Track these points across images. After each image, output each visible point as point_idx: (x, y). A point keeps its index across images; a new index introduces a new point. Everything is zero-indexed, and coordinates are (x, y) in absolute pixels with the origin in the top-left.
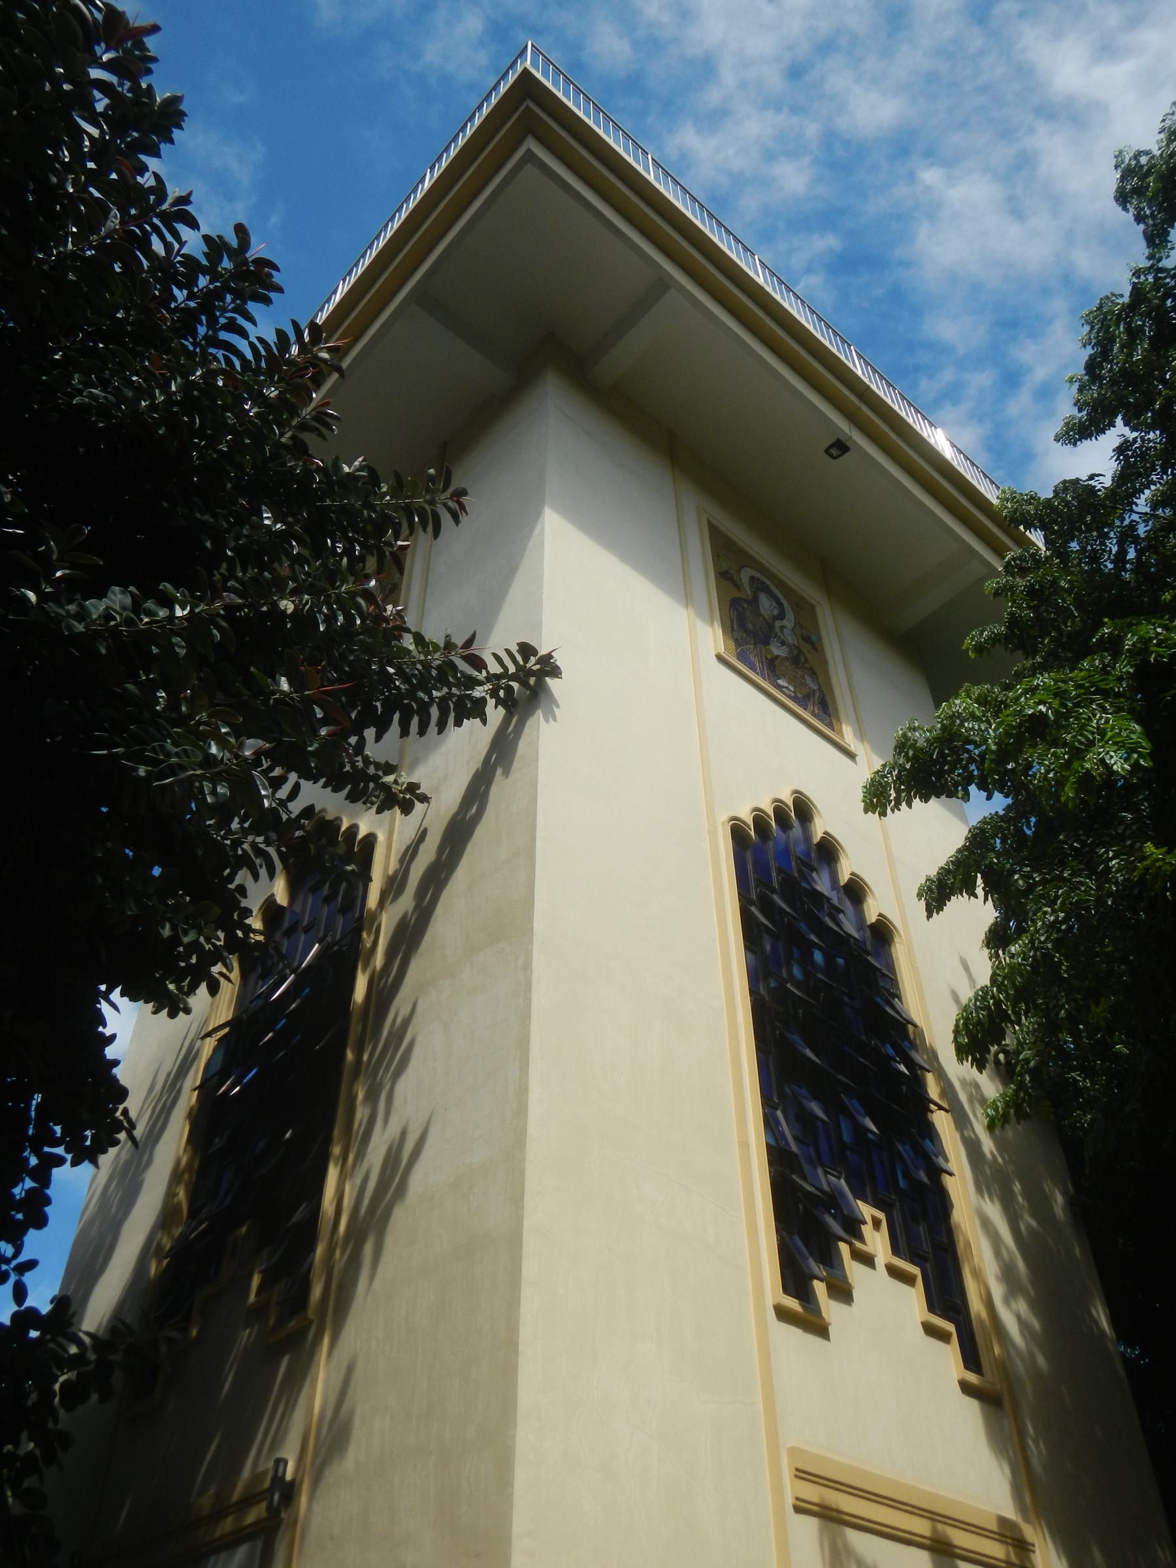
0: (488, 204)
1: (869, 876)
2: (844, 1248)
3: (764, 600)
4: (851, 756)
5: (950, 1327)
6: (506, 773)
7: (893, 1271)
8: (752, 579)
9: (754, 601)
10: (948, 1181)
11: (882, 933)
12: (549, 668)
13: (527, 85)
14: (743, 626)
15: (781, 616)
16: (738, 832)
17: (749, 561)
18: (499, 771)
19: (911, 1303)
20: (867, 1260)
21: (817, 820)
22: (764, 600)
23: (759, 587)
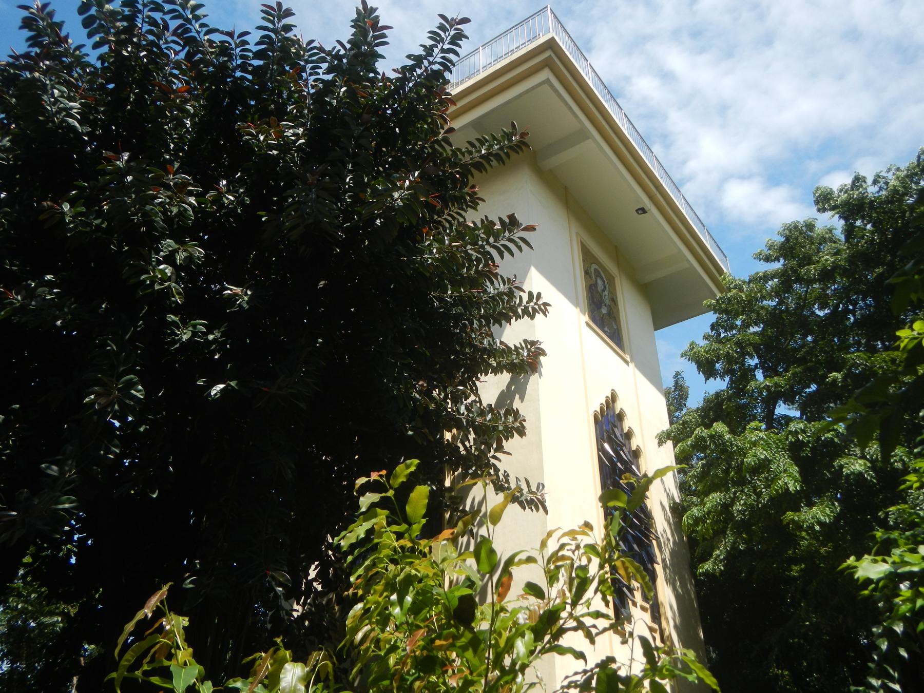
0: (521, 95)
1: (636, 431)
2: (630, 602)
3: (599, 282)
4: (627, 363)
5: (656, 627)
6: (522, 399)
7: (643, 608)
8: (595, 270)
9: (596, 285)
10: (655, 565)
11: (636, 454)
12: (541, 352)
13: (551, 44)
14: (593, 302)
15: (604, 290)
16: (596, 417)
17: (596, 261)
18: (517, 396)
19: (647, 617)
20: (635, 604)
21: (618, 402)
22: (599, 282)
23: (598, 274)
